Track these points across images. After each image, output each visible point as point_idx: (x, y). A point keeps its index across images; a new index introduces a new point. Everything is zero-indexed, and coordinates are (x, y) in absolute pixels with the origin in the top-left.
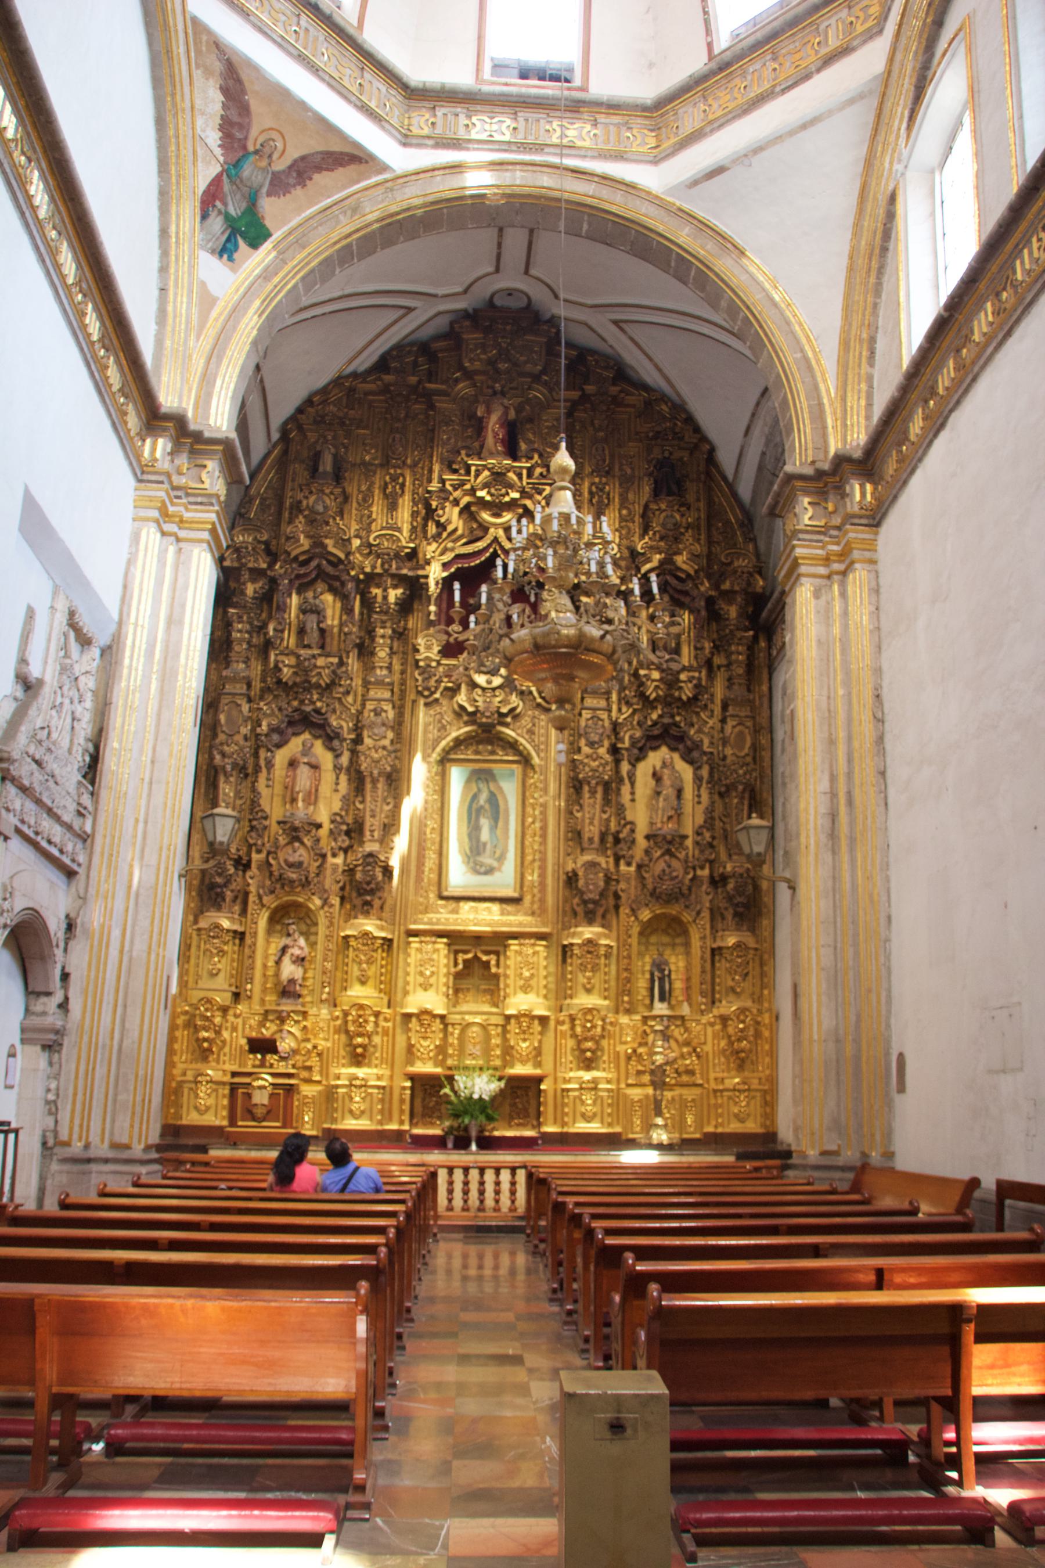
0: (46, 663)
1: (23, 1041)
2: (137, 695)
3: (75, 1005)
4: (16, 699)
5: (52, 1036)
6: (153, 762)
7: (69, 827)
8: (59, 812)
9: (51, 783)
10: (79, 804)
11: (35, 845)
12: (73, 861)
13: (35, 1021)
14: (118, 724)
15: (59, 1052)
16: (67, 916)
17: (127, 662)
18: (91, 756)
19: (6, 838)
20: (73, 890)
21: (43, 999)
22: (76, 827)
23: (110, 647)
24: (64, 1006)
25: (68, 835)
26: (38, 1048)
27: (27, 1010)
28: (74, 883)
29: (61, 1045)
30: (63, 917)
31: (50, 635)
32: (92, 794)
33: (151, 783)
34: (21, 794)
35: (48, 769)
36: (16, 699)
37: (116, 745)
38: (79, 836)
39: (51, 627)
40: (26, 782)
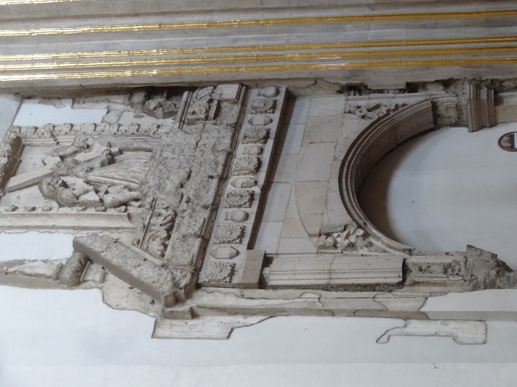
0: (53, 227)
1: (493, 124)
2: (63, 55)
3: (444, 73)
4: (103, 279)
5: (484, 93)
6: (136, 15)
7: (237, 127)
8: (221, 159)
9: (189, 191)
10: (207, 118)
11: (266, 189)
12: (274, 107)
13: (468, 115)
14: (104, 74)
15: (502, 81)
16: (340, 92)
17: (25, 77)
18: (148, 97)
19: (267, 261)
20: (308, 91)
21: (442, 110)
22: (237, 108)
23: (16, 94)
24: (446, 84)
25: (246, 127)
26: (499, 108)
27: (457, 124)
28: (300, 92)
29: (492, 81)
30: (342, 98)
31: (21, 227)
32: (192, 88)
33: (163, 14)
34: (212, 247)
35: (172, 201)
36: (103, 279)
37: (128, 73)
38: (244, 104)
39: (11, 227)
40: (197, 242)
